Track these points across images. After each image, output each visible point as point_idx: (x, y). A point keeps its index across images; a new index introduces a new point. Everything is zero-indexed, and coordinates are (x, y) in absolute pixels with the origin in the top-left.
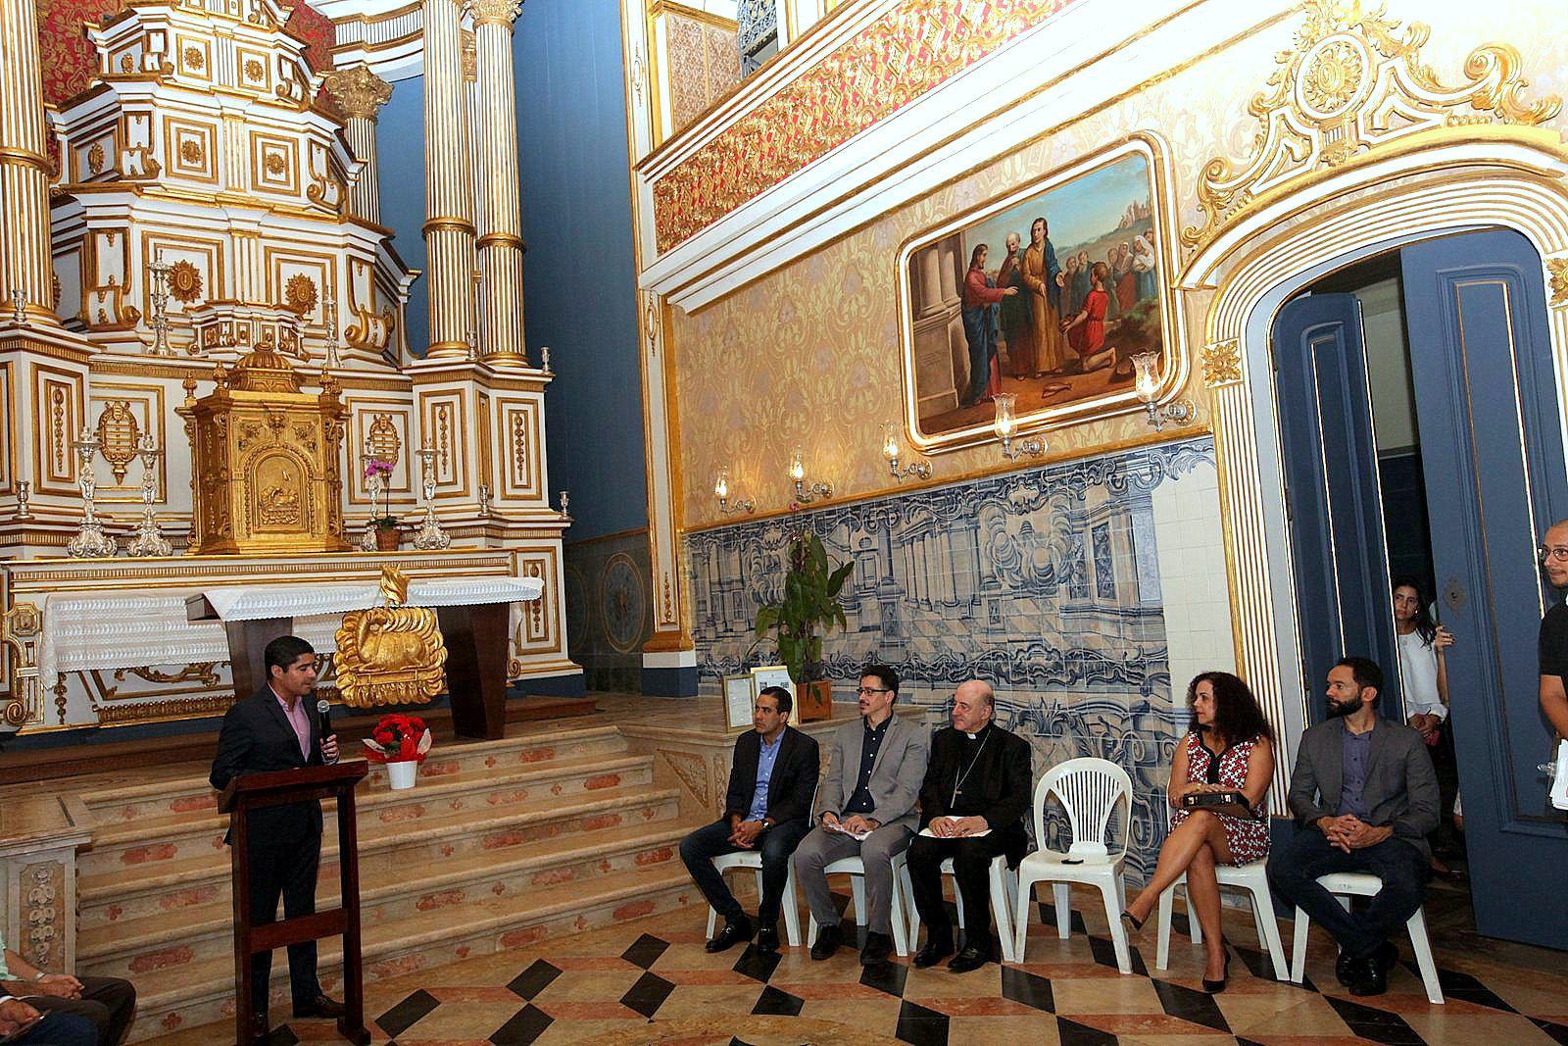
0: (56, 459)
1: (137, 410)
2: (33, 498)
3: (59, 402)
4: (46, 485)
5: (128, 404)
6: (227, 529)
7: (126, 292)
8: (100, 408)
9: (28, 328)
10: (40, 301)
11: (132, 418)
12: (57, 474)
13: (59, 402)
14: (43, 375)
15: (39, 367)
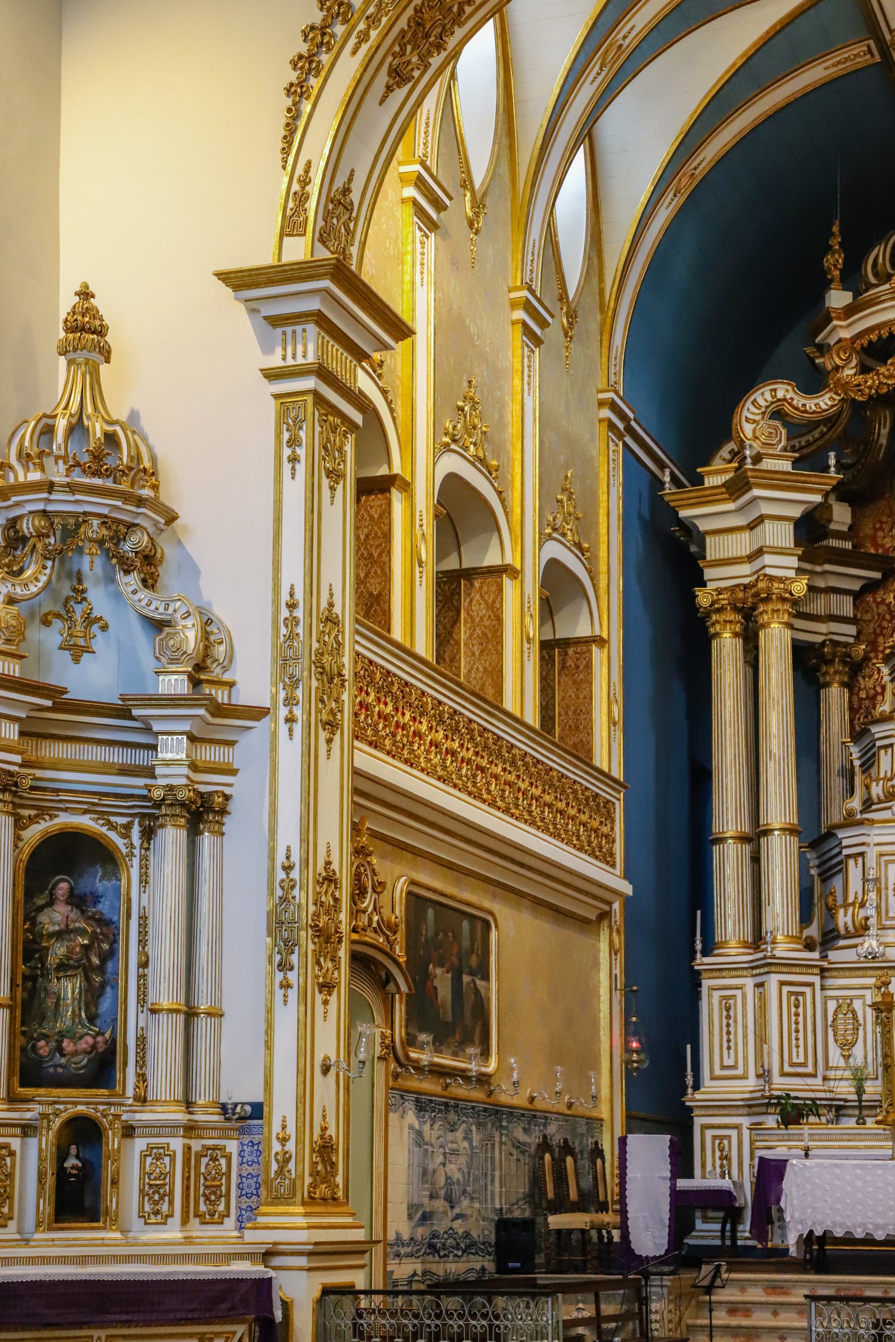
0: (794, 1050)
1: (857, 1005)
2: (777, 1079)
3: (797, 1007)
4: (787, 1069)
5: (851, 1000)
6: (891, 1105)
7: (862, 905)
8: (832, 1006)
9: (773, 957)
10: (788, 932)
11: (854, 1012)
12: (795, 1060)
13: (797, 1007)
14: (785, 989)
15: (782, 983)
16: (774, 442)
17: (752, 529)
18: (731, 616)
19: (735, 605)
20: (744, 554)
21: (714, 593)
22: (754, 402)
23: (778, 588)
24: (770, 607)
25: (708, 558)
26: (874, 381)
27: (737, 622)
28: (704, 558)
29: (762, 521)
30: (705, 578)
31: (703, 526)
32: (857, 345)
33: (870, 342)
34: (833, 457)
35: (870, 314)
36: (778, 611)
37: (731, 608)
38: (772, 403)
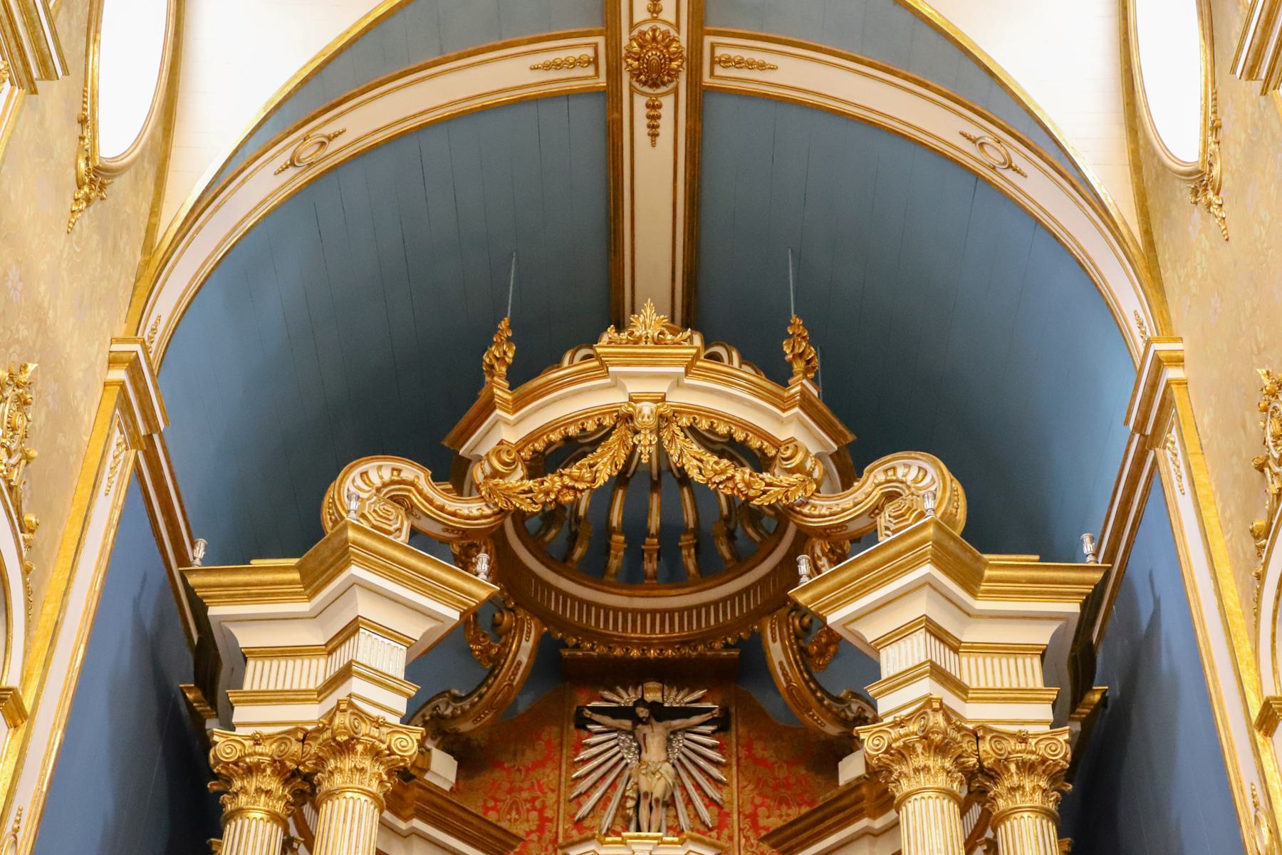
16: (392, 529)
17: (330, 653)
18: (273, 784)
19: (282, 763)
20: (312, 686)
21: (246, 743)
22: (364, 474)
23: (368, 735)
24: (348, 763)
25: (247, 687)
26: (554, 483)
27: (280, 798)
28: (240, 685)
29: (357, 630)
30: (235, 720)
31: (246, 638)
32: (526, 454)
33: (550, 444)
34: (485, 560)
35: (554, 401)
36: (362, 770)
37: (273, 772)
38: (393, 482)
